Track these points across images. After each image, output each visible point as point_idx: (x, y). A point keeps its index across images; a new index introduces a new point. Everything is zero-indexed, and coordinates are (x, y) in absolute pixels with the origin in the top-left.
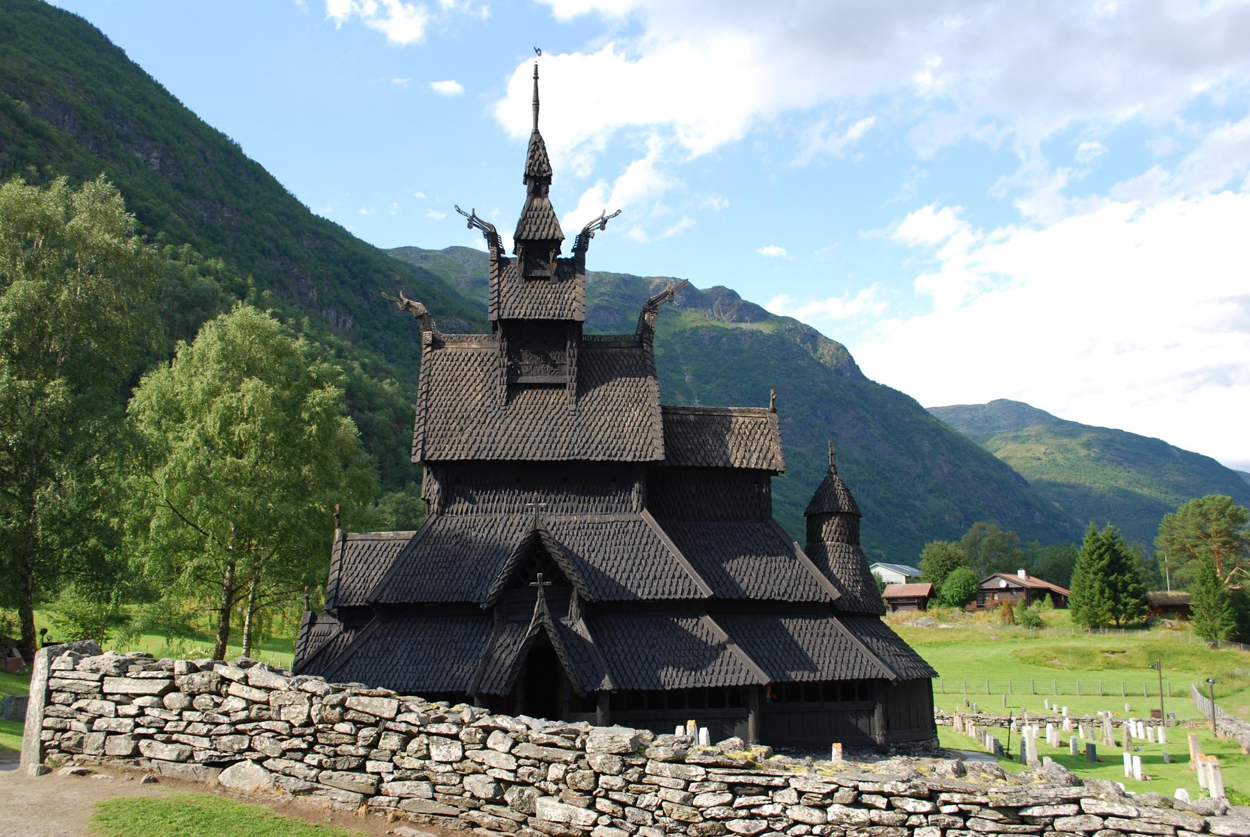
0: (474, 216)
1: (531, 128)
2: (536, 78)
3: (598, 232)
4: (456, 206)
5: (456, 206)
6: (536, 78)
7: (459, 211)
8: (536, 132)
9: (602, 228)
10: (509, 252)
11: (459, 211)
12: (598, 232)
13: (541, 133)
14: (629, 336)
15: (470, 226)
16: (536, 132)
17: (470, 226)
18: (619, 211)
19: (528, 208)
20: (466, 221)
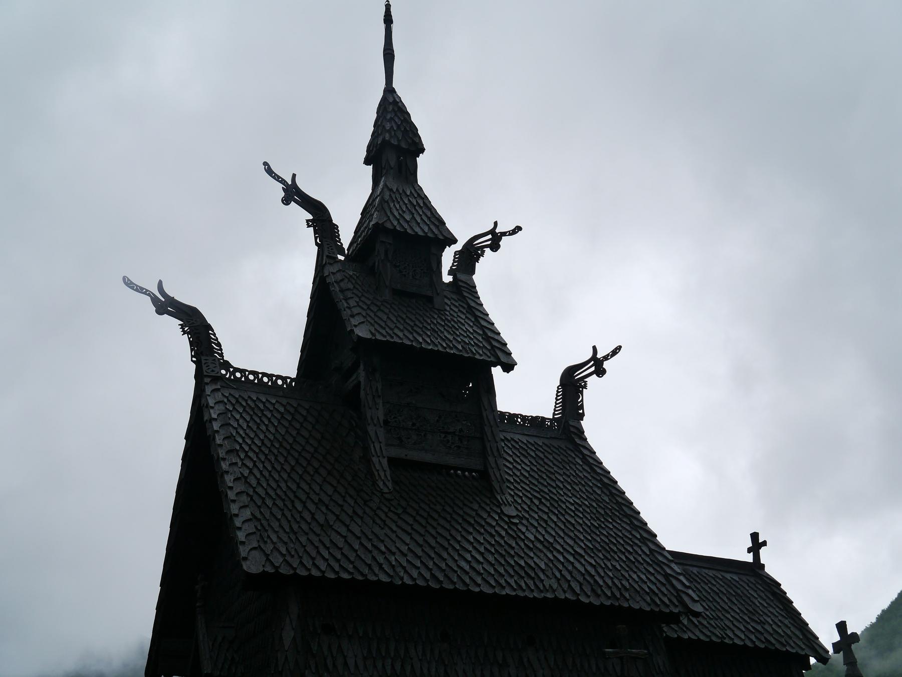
2: (388, 20)
3: (487, 250)
4: (265, 164)
5: (265, 164)
6: (388, 20)
7: (269, 171)
8: (389, 90)
9: (495, 247)
11: (269, 171)
13: (399, 92)
14: (544, 419)
15: (286, 201)
16: (389, 90)
17: (286, 201)
18: (518, 229)
20: (278, 191)
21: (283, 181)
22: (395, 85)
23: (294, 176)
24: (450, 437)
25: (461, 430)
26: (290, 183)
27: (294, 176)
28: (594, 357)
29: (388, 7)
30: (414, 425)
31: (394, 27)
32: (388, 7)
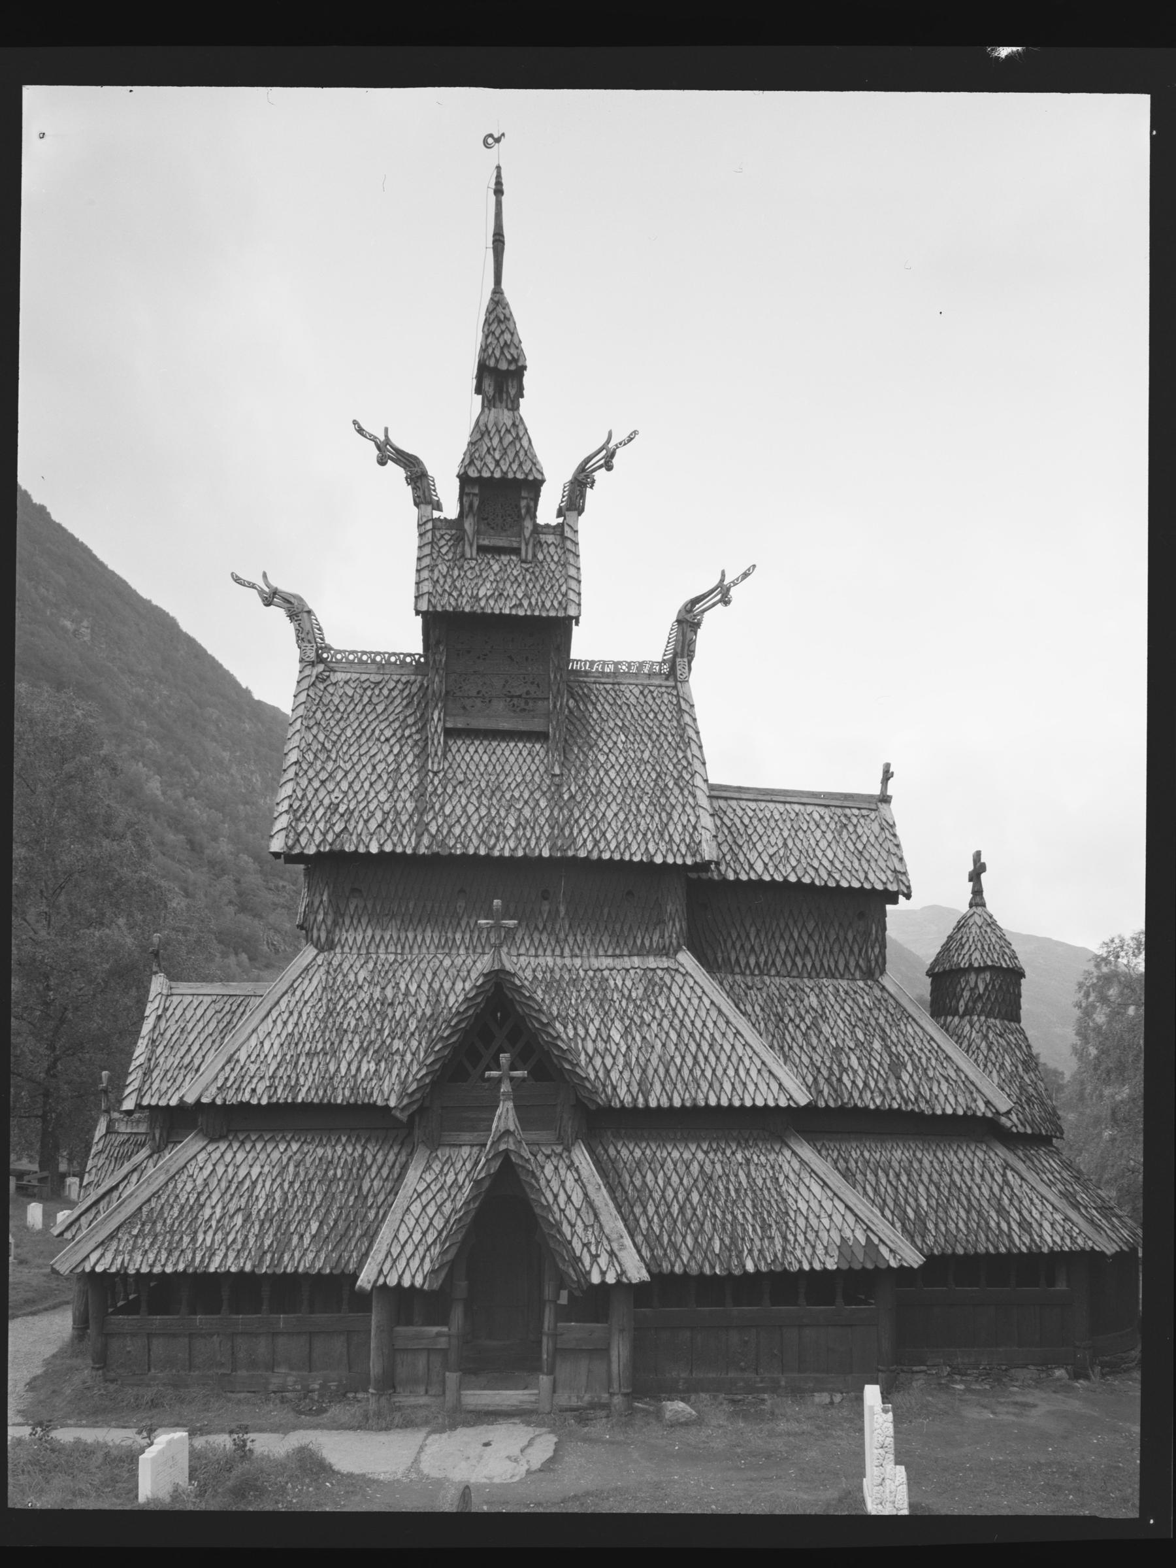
0: (387, 441)
1: (491, 286)
2: (499, 191)
4: (355, 422)
5: (355, 422)
6: (499, 191)
7: (360, 431)
8: (497, 290)
10: (450, 509)
11: (360, 431)
12: (600, 475)
16: (497, 290)
19: (481, 432)
21: (373, 439)
22: (505, 286)
23: (386, 430)
24: (515, 701)
25: (528, 693)
26: (382, 438)
27: (386, 430)
28: (721, 584)
29: (498, 168)
30: (478, 693)
31: (505, 199)
32: (498, 168)
